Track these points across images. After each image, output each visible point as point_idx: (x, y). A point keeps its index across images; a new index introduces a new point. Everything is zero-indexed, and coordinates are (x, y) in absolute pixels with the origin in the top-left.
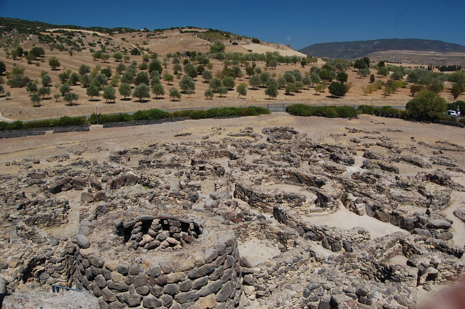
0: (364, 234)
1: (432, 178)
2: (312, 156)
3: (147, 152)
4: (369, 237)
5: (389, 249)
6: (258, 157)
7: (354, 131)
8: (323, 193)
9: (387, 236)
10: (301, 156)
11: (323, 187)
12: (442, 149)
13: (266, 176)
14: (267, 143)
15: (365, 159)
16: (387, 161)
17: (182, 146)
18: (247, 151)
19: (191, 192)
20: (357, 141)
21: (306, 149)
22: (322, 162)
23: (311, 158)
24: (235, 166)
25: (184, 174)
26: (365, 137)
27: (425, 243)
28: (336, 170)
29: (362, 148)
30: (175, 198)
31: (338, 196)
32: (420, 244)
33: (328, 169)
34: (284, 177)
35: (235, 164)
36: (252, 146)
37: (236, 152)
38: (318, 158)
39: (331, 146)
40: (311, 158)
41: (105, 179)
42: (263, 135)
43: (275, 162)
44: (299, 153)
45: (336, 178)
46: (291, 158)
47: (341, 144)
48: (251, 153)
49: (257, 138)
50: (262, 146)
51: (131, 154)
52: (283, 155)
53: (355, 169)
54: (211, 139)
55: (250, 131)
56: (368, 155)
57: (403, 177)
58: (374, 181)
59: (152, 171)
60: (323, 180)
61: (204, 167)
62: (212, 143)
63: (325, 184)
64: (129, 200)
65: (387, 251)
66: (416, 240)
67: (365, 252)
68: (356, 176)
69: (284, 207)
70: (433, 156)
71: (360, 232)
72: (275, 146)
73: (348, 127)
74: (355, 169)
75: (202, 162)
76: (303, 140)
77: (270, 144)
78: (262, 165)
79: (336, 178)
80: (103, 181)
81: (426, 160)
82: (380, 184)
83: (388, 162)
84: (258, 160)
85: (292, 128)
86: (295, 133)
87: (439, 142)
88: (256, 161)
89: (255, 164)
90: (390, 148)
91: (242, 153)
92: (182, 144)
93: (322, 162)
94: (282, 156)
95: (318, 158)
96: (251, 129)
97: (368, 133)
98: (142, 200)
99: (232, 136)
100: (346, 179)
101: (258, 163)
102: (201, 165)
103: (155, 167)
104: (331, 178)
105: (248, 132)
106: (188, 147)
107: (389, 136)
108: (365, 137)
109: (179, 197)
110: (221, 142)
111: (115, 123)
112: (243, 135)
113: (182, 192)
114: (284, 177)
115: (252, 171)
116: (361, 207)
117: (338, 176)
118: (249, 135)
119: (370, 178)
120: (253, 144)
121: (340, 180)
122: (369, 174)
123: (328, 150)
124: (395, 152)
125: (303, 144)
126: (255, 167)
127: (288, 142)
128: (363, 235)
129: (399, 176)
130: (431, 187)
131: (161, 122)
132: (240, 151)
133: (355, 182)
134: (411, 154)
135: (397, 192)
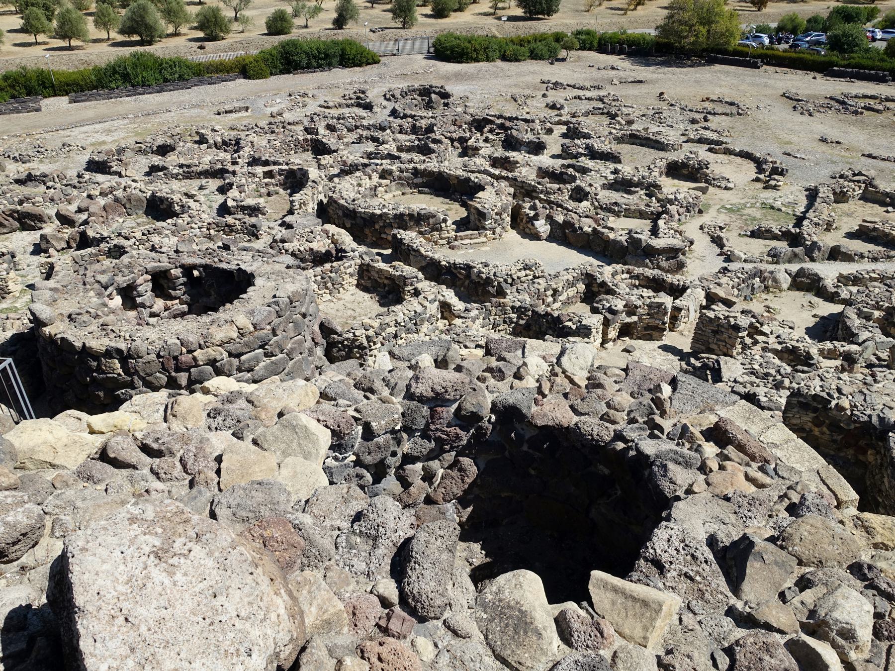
1: (675, 170)
2: (473, 140)
3: (164, 150)
6: (370, 147)
7: (557, 85)
8: (478, 206)
10: (452, 140)
11: (480, 194)
12: (710, 113)
13: (384, 182)
14: (391, 119)
15: (567, 141)
16: (602, 142)
17: (233, 133)
18: (352, 137)
19: (247, 219)
20: (558, 106)
21: (464, 126)
22: (486, 150)
23: (469, 143)
24: (331, 166)
25: (234, 187)
26: (575, 98)
28: (510, 162)
29: (564, 119)
30: (218, 231)
31: (504, 209)
33: (496, 162)
34: (415, 181)
35: (331, 161)
36: (363, 126)
37: (332, 139)
38: (481, 144)
39: (511, 119)
40: (469, 143)
41: (84, 205)
42: (385, 103)
43: (403, 155)
44: (449, 134)
45: (506, 178)
46: (432, 145)
47: (528, 113)
48: (360, 140)
49: (375, 109)
50: (383, 125)
51: (132, 153)
52: (419, 140)
53: (545, 160)
54: (288, 116)
55: (362, 96)
56: (573, 133)
57: (627, 170)
58: (574, 179)
59: (175, 185)
60: (482, 183)
61: (271, 171)
62: (289, 124)
63: (483, 189)
64: (133, 240)
68: (543, 173)
69: (409, 236)
70: (690, 127)
72: (407, 123)
73: (546, 79)
74: (545, 160)
75: (266, 163)
76: (460, 109)
77: (399, 121)
78: (379, 162)
79: (506, 178)
80: (80, 210)
81: (672, 136)
82: (583, 185)
83: (607, 143)
84: (371, 153)
85: (442, 87)
86: (445, 95)
87: (708, 99)
88: (369, 156)
89: (366, 161)
90: (613, 116)
91: (345, 140)
92: (231, 129)
93: (486, 150)
94: (417, 143)
95: (481, 144)
96: (363, 92)
97: (582, 88)
98: (156, 239)
99: (328, 107)
100: (524, 180)
101: (370, 159)
102: (266, 169)
103: (180, 177)
104: (498, 178)
105: (358, 98)
106: (242, 135)
107: (618, 94)
108: (575, 98)
109: (227, 229)
110: (306, 122)
111: (95, 91)
112: (348, 106)
113: (229, 219)
114: (415, 181)
115: (358, 174)
116: (542, 226)
117: (510, 175)
118: (359, 105)
119: (566, 173)
120: (365, 123)
121: (513, 182)
122: (569, 166)
123: (502, 127)
124: (624, 123)
125: (457, 117)
126: (365, 166)
127: (430, 114)
129: (619, 167)
130: (669, 186)
131: (189, 85)
132: (340, 138)
133: (539, 183)
134: (649, 125)
135: (607, 196)
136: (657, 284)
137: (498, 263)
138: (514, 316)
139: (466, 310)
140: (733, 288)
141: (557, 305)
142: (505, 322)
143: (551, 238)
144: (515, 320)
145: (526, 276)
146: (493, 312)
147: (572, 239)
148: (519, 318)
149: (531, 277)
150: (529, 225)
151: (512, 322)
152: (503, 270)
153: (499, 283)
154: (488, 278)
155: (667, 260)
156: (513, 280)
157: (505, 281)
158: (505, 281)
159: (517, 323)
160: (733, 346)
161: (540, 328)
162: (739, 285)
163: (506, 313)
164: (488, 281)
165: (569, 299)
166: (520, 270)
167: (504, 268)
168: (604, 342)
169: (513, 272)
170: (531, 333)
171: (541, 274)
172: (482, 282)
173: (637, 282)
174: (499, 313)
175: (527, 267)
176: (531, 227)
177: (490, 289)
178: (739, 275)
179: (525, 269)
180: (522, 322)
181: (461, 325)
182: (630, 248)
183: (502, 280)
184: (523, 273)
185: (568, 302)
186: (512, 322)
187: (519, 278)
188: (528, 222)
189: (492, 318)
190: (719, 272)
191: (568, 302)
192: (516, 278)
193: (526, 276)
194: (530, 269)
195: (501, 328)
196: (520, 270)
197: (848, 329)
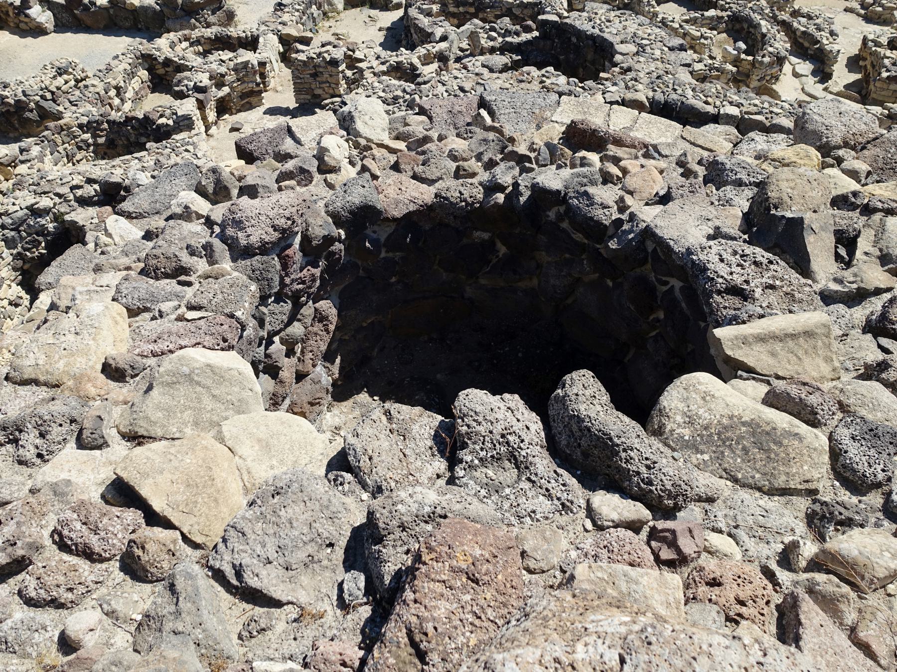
0: (70, 70)
4: (84, 74)
5: (132, 82)
9: (117, 57)
27: (192, 45)
32: (184, 50)
65: (130, 88)
66: (172, 46)
67: (89, 107)
71: (61, 72)
128: (71, 73)
136: (223, 44)
137: (19, 78)
138: (87, 136)
139: (22, 151)
140: (297, 23)
141: (127, 106)
142: (80, 148)
143: (61, 27)
144: (90, 141)
145: (66, 82)
146: (59, 141)
147: (88, 21)
148: (94, 136)
149: (73, 83)
150: (22, 18)
151: (89, 145)
152: (33, 85)
153: (37, 103)
154: (18, 102)
155: (213, 13)
156: (53, 93)
157: (42, 97)
158: (42, 97)
159: (96, 144)
160: (337, 84)
161: (128, 140)
162: (301, 19)
163: (75, 137)
164: (20, 106)
165: (137, 93)
166: (54, 77)
167: (32, 81)
168: (207, 128)
169: (47, 83)
170: (119, 149)
171: (83, 75)
172: (12, 110)
173: (201, 49)
174: (67, 139)
175: (61, 72)
176: (26, 20)
177: (28, 114)
178: (297, 7)
179: (60, 75)
180: (101, 140)
181: (29, 171)
182: (166, 10)
183: (38, 98)
184: (60, 81)
185: (138, 99)
186: (89, 145)
187: (58, 88)
188: (18, 15)
189: (60, 149)
190: (276, 10)
191: (138, 99)
192: (55, 90)
193: (66, 82)
194: (66, 72)
195: (79, 156)
196: (54, 77)
197: (421, 30)
